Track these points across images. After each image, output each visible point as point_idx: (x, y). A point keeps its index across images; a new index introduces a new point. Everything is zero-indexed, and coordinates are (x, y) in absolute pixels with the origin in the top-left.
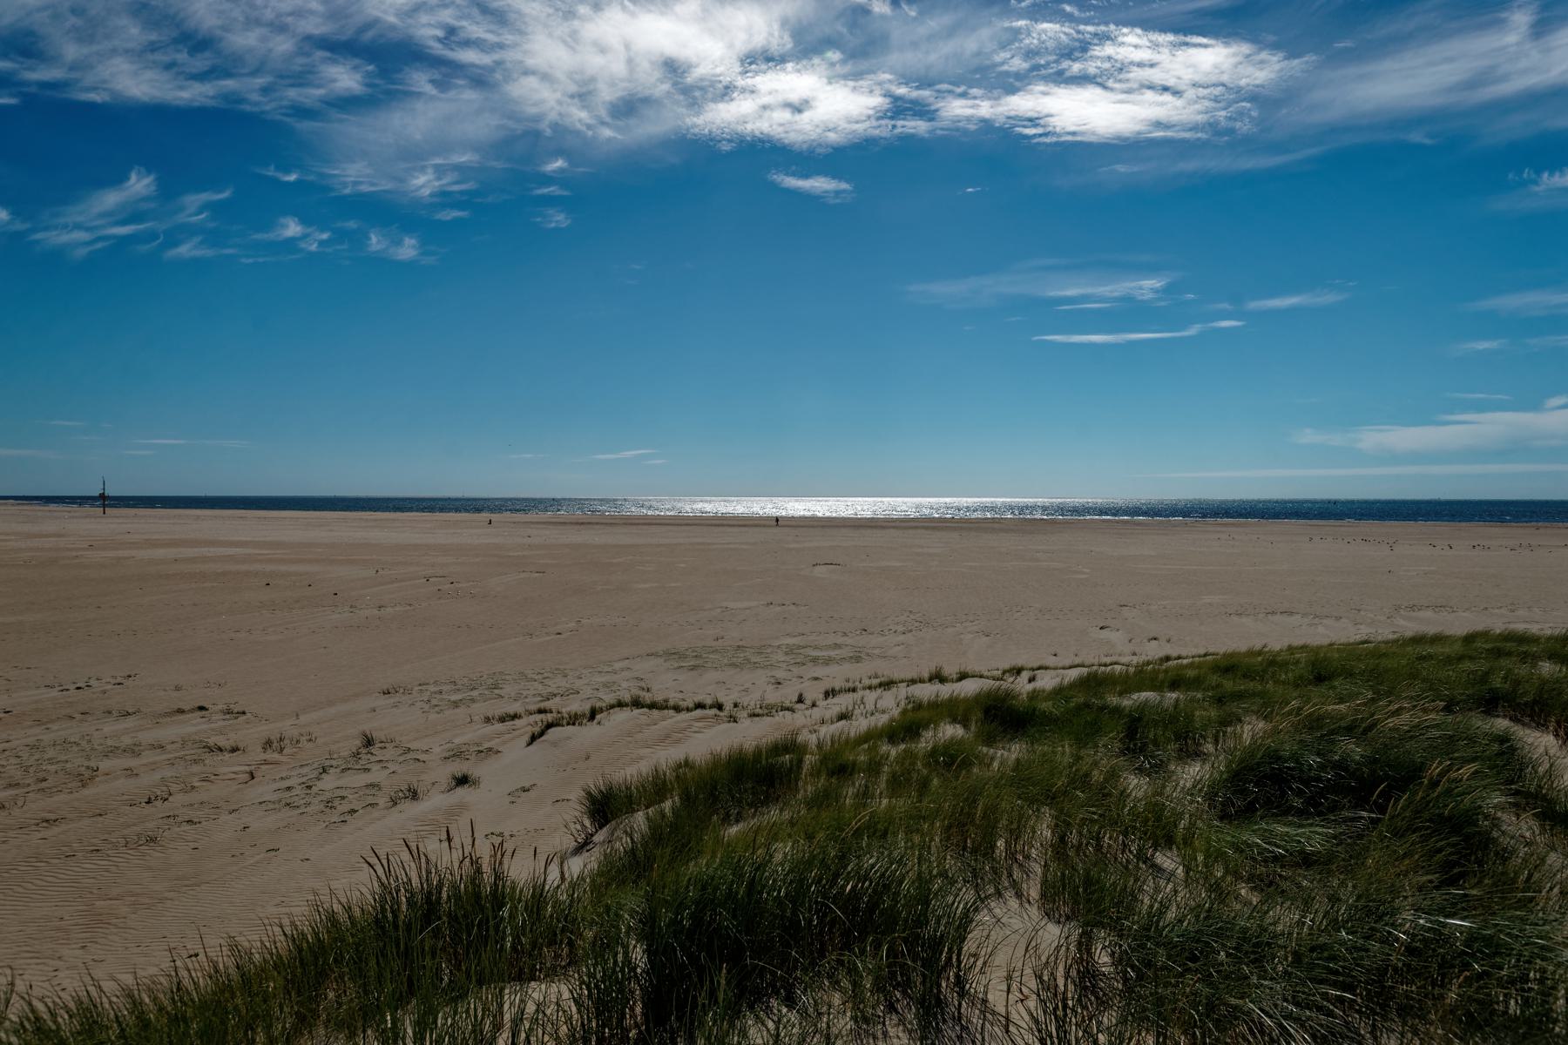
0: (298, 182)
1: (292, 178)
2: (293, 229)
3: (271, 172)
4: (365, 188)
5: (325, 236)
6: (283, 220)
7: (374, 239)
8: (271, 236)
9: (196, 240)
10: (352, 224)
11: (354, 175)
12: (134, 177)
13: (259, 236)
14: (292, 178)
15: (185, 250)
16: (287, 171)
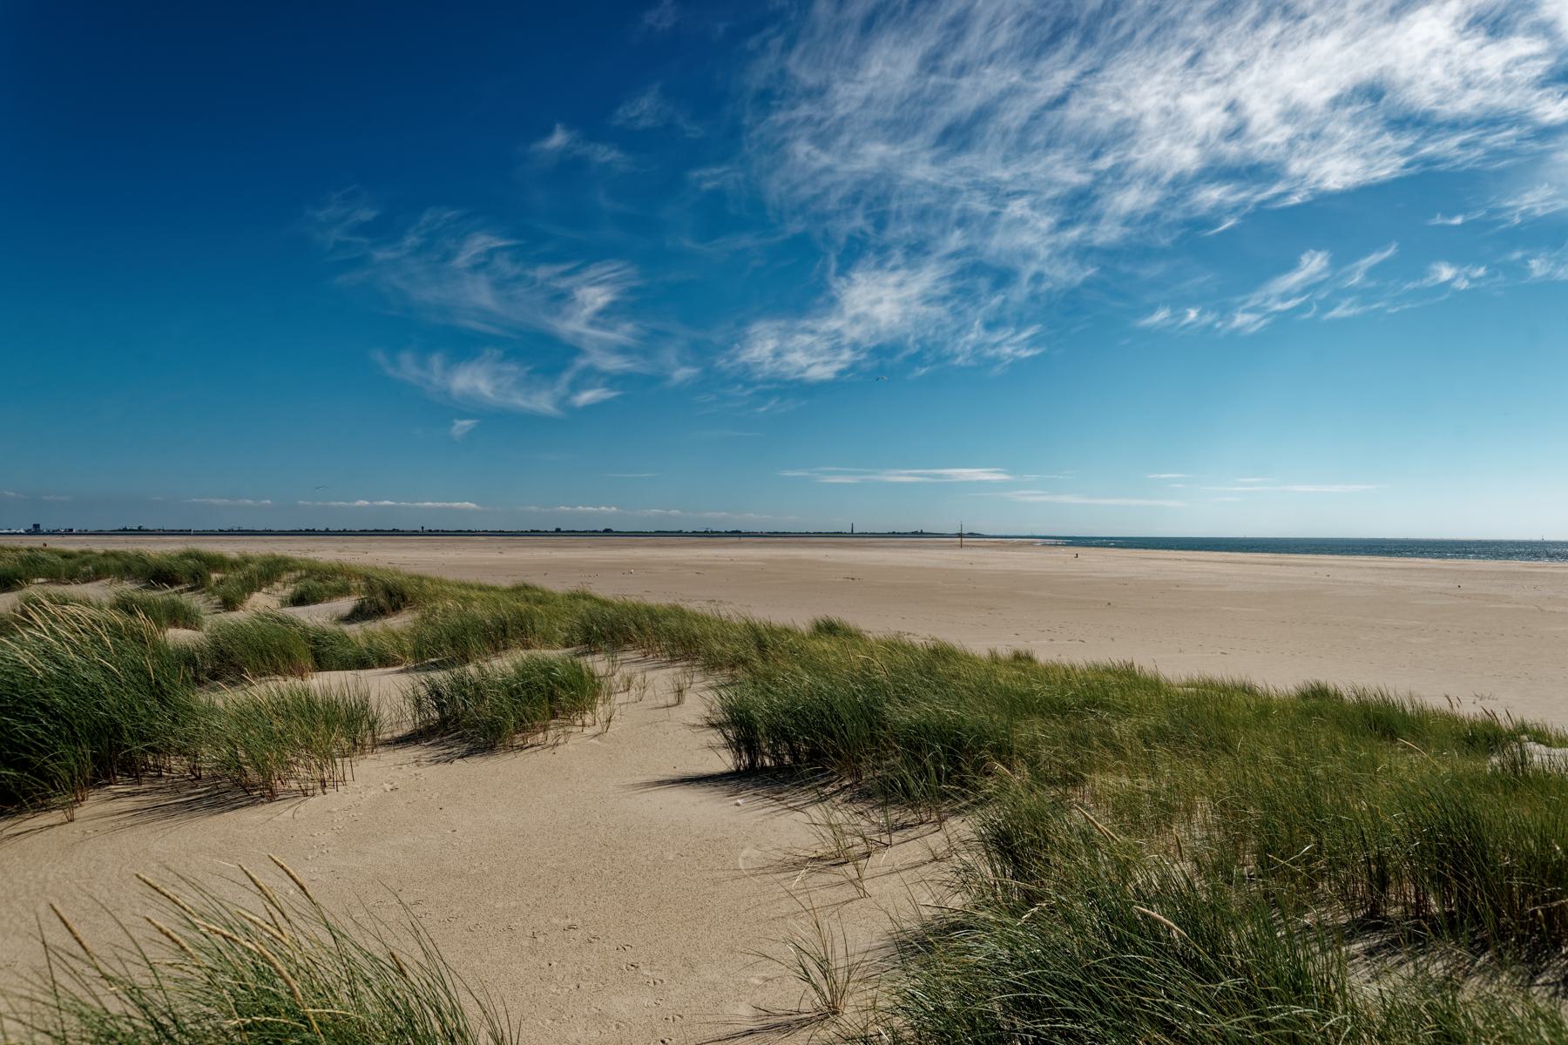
0: (1463, 225)
1: (1458, 220)
2: (1446, 273)
3: (1438, 220)
4: (1539, 212)
5: (1481, 271)
6: (1434, 267)
7: (1534, 263)
8: (1427, 282)
9: (1350, 300)
10: (1517, 255)
11: (1534, 200)
12: (1305, 259)
13: (1411, 285)
14: (1458, 220)
15: (1339, 312)
16: (1452, 215)
